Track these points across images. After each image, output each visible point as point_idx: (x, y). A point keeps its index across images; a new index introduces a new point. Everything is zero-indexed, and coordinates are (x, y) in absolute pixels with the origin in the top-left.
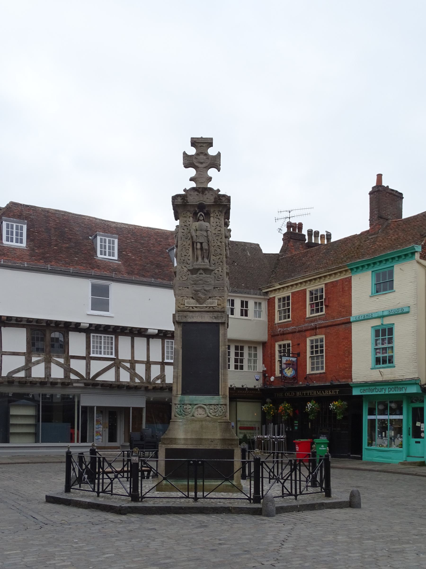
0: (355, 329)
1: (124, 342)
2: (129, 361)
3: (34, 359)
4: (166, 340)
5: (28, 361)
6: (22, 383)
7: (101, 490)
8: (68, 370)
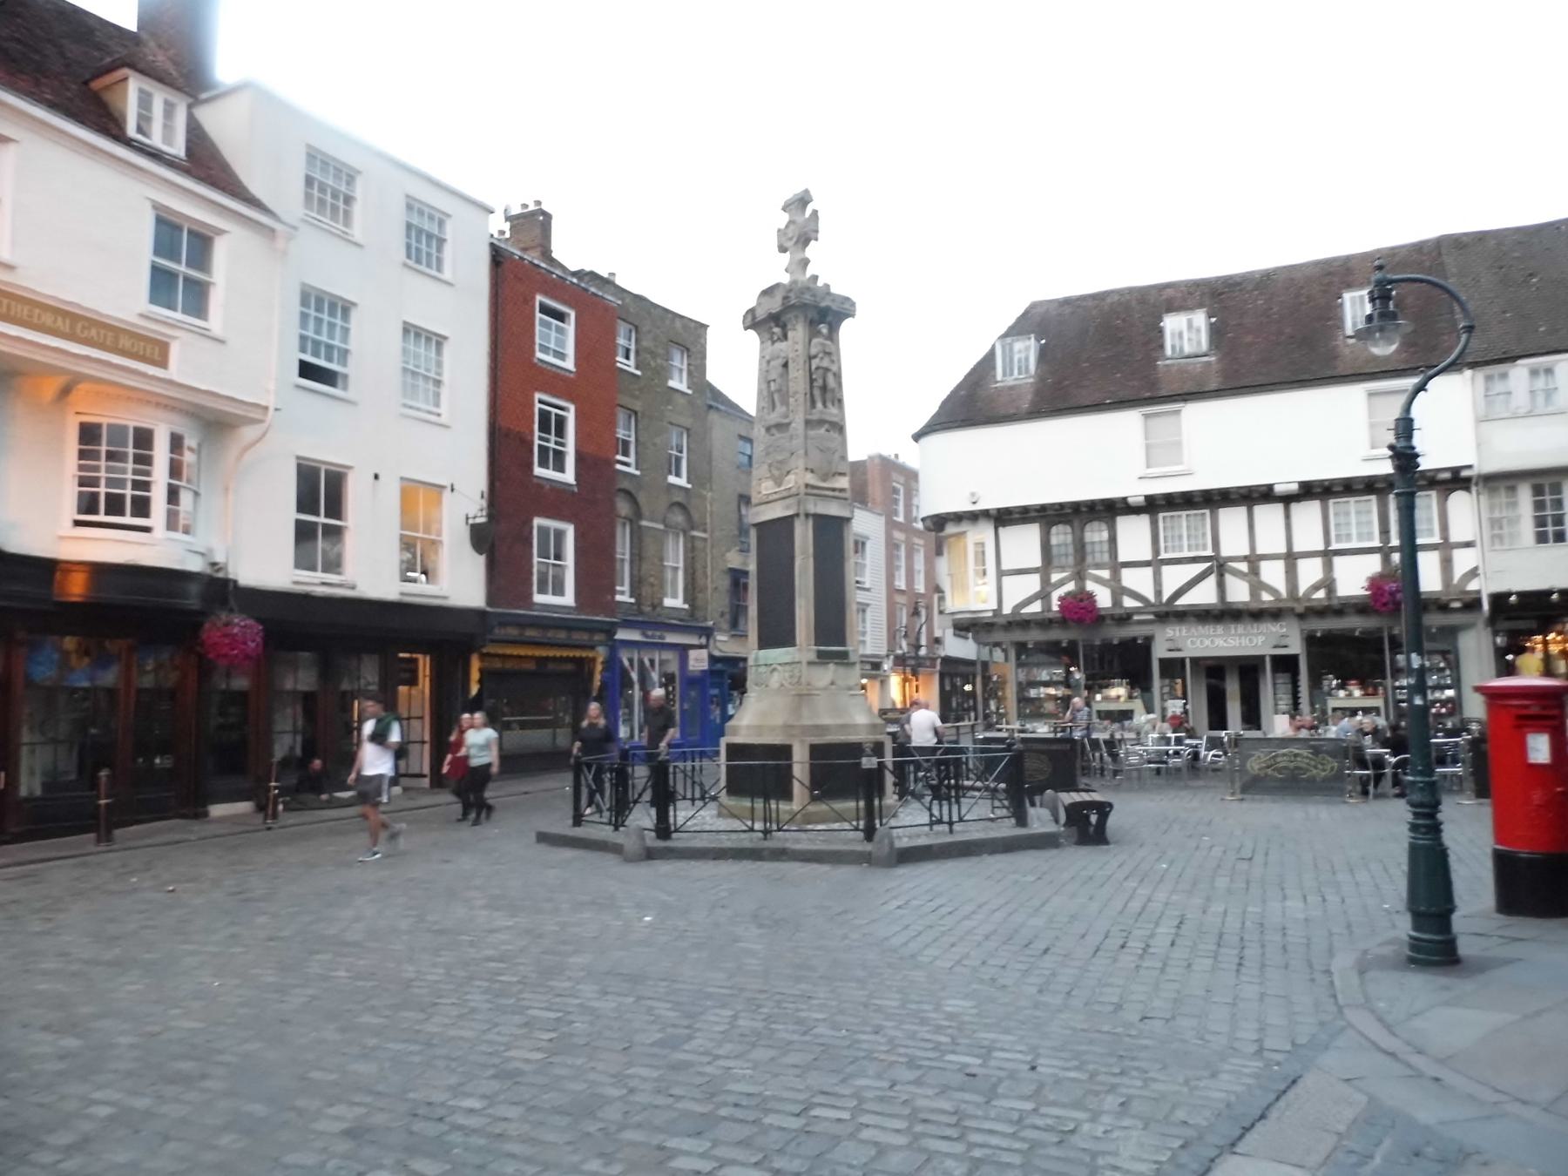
1: (1232, 520)
2: (1245, 558)
4: (1331, 502)
5: (1045, 581)
6: (1044, 623)
8: (1119, 591)
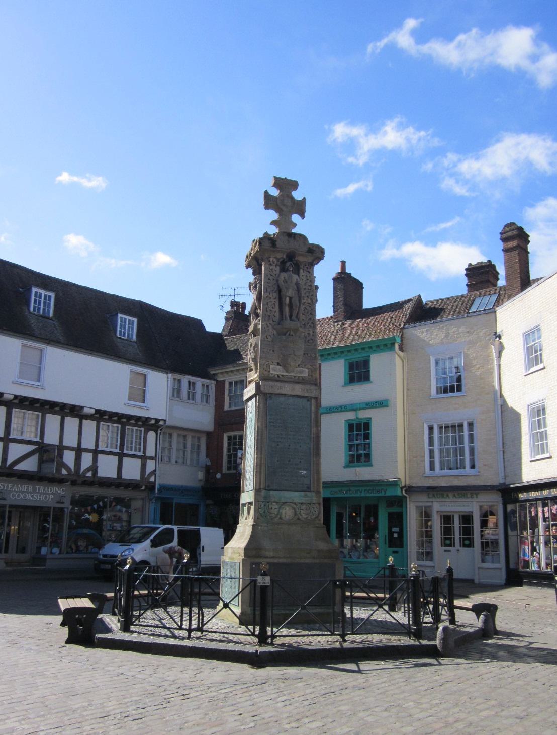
0: (325, 420)
7: (194, 626)
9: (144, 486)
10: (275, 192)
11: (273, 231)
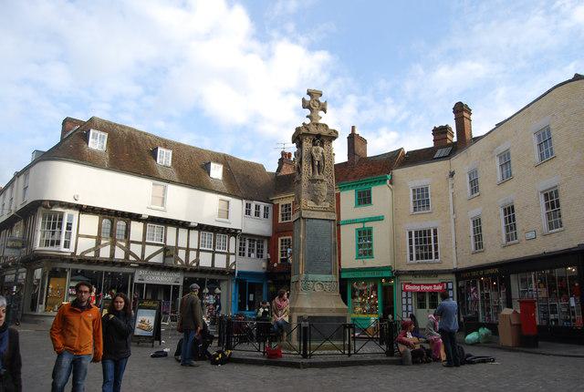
1: (171, 231)
3: (103, 242)
5: (98, 243)
6: (89, 261)
8: (128, 253)
9: (226, 273)
10: (308, 98)
11: (308, 121)
